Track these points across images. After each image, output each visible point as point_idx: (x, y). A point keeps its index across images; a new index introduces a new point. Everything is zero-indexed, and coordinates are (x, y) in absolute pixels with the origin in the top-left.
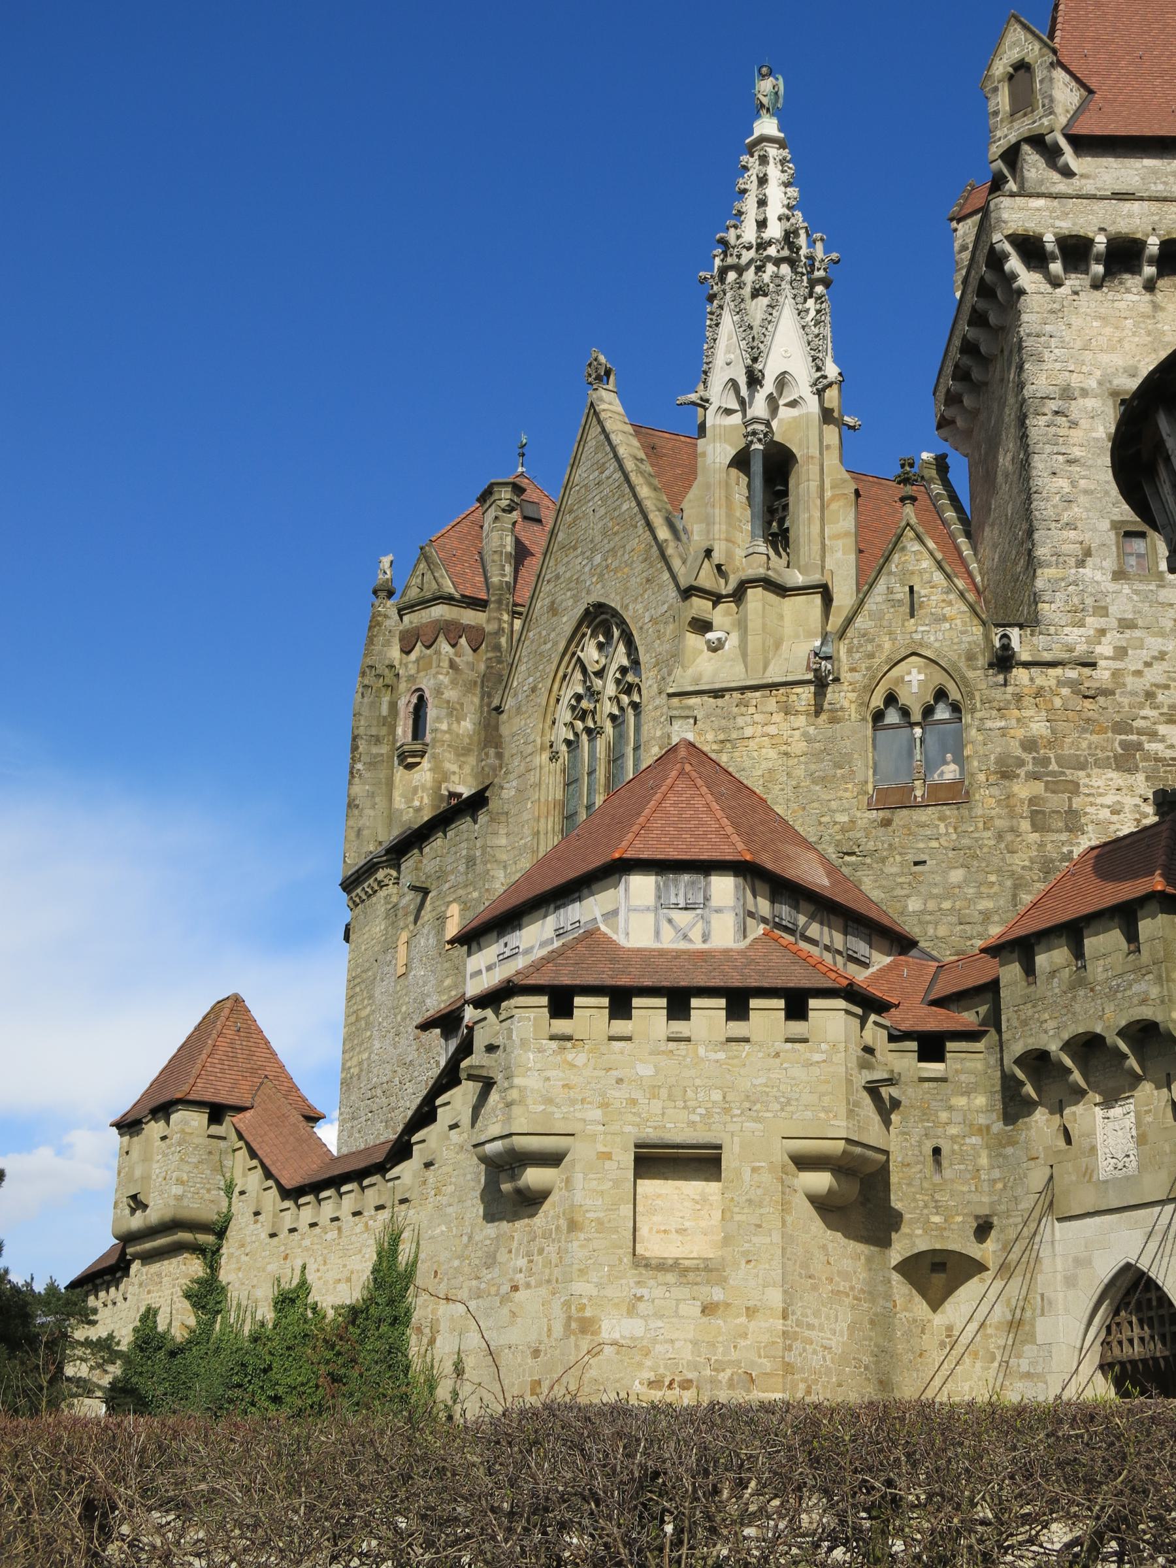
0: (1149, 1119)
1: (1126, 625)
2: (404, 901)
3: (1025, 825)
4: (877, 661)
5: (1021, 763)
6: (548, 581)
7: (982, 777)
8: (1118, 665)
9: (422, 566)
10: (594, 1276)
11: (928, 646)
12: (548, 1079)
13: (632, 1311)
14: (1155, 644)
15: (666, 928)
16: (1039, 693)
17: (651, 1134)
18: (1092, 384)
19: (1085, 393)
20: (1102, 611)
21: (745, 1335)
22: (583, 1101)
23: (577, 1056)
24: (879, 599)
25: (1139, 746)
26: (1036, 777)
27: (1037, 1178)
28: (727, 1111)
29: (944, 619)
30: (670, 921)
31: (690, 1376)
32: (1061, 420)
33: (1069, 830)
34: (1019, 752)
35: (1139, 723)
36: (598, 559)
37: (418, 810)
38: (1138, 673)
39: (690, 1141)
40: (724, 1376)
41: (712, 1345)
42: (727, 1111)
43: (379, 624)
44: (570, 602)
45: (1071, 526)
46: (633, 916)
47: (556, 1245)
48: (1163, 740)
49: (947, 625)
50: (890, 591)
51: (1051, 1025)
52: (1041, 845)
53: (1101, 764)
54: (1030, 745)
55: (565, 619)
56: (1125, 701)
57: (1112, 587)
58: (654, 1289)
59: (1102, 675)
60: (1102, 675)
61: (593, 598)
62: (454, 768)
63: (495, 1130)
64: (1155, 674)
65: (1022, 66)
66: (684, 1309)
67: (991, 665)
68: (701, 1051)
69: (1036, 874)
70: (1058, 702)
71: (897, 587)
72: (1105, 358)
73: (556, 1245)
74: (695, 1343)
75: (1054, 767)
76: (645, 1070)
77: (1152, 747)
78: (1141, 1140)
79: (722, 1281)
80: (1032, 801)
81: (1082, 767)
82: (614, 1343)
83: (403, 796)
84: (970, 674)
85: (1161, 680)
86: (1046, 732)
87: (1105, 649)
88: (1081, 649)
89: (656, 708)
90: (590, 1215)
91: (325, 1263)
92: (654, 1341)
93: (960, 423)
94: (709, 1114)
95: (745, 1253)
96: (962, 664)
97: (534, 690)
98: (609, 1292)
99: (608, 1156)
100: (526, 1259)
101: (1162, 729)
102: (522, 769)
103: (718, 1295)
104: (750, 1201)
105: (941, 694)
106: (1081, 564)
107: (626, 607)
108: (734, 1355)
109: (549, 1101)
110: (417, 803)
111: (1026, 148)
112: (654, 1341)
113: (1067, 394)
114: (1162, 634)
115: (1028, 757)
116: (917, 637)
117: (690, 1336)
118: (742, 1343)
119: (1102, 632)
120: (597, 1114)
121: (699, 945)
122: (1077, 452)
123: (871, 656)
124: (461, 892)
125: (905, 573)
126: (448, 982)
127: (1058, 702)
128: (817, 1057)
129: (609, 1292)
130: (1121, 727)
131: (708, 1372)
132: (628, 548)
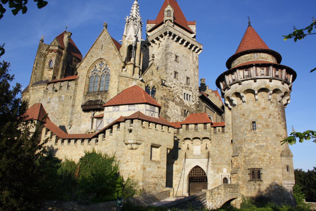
0: (203, 149)
1: (174, 84)
2: (49, 92)
3: (163, 106)
4: (147, 80)
5: (163, 98)
6: (91, 52)
7: (159, 98)
8: (173, 89)
9: (55, 40)
10: (145, 162)
11: (154, 80)
12: (141, 133)
13: (150, 167)
14: (177, 87)
15: (150, 113)
16: (166, 90)
17: (153, 142)
18: (173, 53)
19: (173, 54)
20: (172, 81)
21: (162, 171)
22: (145, 137)
23: (145, 130)
24: (148, 72)
25: (175, 99)
26: (164, 100)
27: (183, 153)
28: (161, 141)
29: (156, 77)
30: (151, 113)
31: (156, 176)
32: (170, 56)
33: (167, 108)
34: (163, 97)
35: (175, 96)
36: (103, 52)
37: (50, 78)
38: (175, 90)
39: (156, 144)
40: (160, 177)
41: (159, 173)
42: (161, 141)
43: (41, 46)
44: (96, 56)
45: (170, 70)
46: (146, 111)
47: (139, 157)
48: (177, 99)
49: (156, 78)
50: (150, 71)
51: (191, 135)
52: (164, 109)
53: (171, 100)
54: (164, 96)
55: (94, 58)
56: (174, 93)
57: (174, 79)
58: (153, 164)
59: (172, 89)
60: (172, 89)
61: (101, 57)
62: (56, 73)
63: (132, 139)
64: (177, 91)
65: (169, 11)
66: (156, 167)
67: (161, 85)
68: (159, 132)
69: (163, 112)
70: (167, 91)
71: (151, 71)
72: (175, 50)
73: (139, 157)
74: (157, 172)
75: (166, 99)
76: (152, 134)
77: (176, 100)
78: (201, 151)
79: (160, 164)
80: (164, 103)
81: (169, 100)
82: (148, 171)
83: (47, 74)
84: (158, 85)
85: (177, 92)
86: (166, 95)
87: (172, 86)
88: (170, 86)
89: (115, 77)
90: (145, 153)
91: (72, 152)
92: (152, 171)
93: (144, 49)
94: (159, 141)
95: (163, 160)
96: (158, 83)
97: (86, 67)
98: (147, 164)
99: (148, 145)
100: (130, 158)
101: (177, 98)
102: (82, 78)
103: (159, 166)
104: (163, 153)
105: (154, 86)
106: (171, 75)
107: (109, 61)
108: (161, 174)
109: (141, 136)
110: (49, 76)
111: (169, 21)
112: (152, 171)
113: (171, 53)
114: (178, 86)
115: (164, 97)
116: (153, 78)
117: (156, 171)
118: (162, 172)
119: (172, 84)
120: (146, 139)
121: (154, 117)
122: (172, 61)
123: (147, 79)
124: (65, 93)
125: (152, 70)
126: (60, 107)
127: (167, 91)
128: (171, 135)
129: (147, 164)
130: (173, 97)
131: (158, 176)
132: (110, 52)
